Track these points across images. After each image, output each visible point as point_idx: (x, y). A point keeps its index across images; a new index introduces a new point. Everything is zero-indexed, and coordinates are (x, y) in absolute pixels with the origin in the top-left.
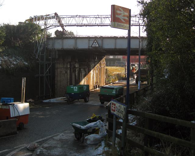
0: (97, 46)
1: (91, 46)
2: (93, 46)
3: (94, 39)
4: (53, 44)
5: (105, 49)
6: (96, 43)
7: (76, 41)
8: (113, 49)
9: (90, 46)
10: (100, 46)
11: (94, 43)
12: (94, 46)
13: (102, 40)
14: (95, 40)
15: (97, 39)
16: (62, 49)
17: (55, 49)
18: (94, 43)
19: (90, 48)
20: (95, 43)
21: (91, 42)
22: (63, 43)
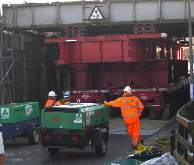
0: (100, 17)
1: (89, 19)
2: (92, 18)
3: (94, 6)
4: (15, 19)
5: (116, 22)
6: (98, 13)
7: (59, 10)
8: (130, 22)
9: (87, 18)
10: (106, 17)
11: (94, 13)
12: (94, 18)
13: (109, 6)
14: (96, 6)
15: (98, 5)
16: (32, 26)
17: (18, 26)
18: (94, 12)
19: (87, 22)
20: (96, 12)
21: (88, 12)
22: (33, 15)
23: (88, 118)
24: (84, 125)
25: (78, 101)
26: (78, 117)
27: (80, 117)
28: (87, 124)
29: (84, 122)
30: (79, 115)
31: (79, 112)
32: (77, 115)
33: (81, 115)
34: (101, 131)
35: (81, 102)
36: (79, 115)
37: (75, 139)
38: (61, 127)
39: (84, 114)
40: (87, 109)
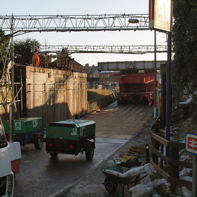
23: (81, 132)
24: (78, 136)
25: (74, 118)
26: (74, 131)
27: (75, 131)
28: (80, 136)
29: (78, 135)
30: (75, 129)
31: (75, 127)
32: (74, 129)
33: (76, 129)
34: (90, 141)
35: (75, 119)
36: (75, 129)
37: (71, 147)
38: (61, 138)
39: (79, 129)
40: (81, 125)
